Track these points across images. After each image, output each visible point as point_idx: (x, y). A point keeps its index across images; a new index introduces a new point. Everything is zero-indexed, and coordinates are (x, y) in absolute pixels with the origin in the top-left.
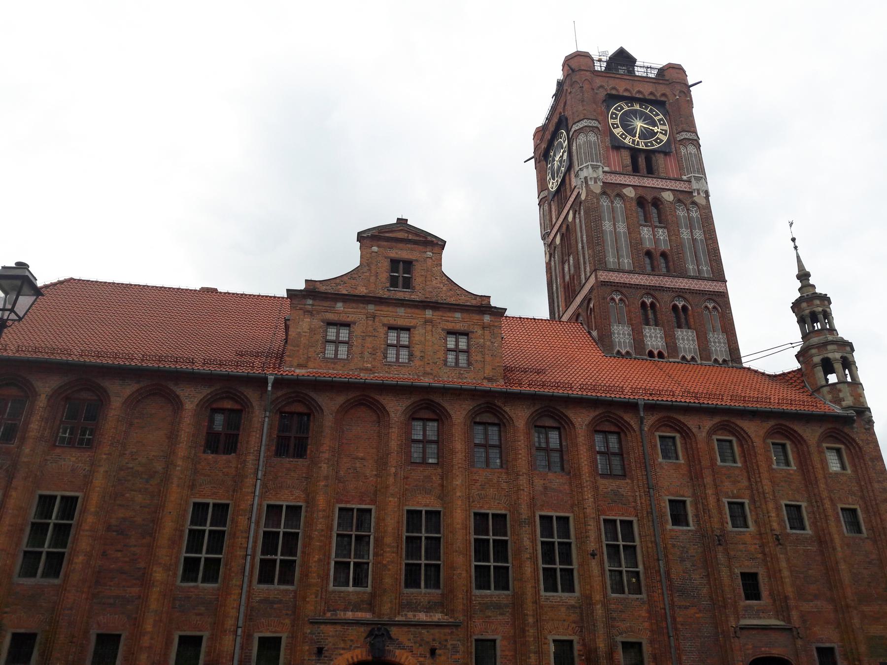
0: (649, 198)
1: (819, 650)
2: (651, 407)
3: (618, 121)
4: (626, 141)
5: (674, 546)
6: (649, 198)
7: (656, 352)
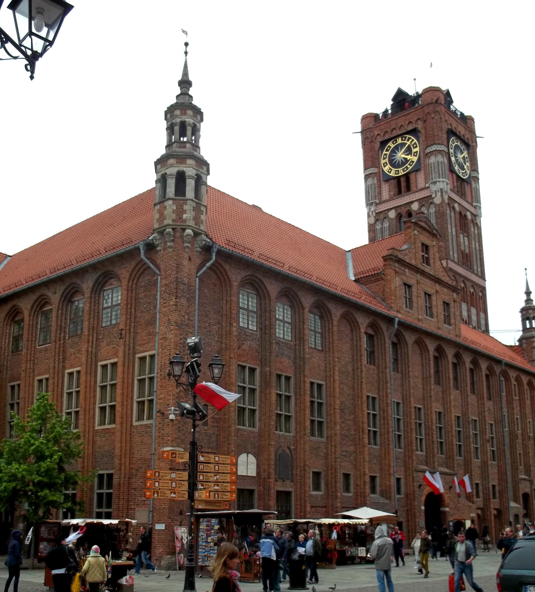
3: (387, 160)
4: (391, 174)
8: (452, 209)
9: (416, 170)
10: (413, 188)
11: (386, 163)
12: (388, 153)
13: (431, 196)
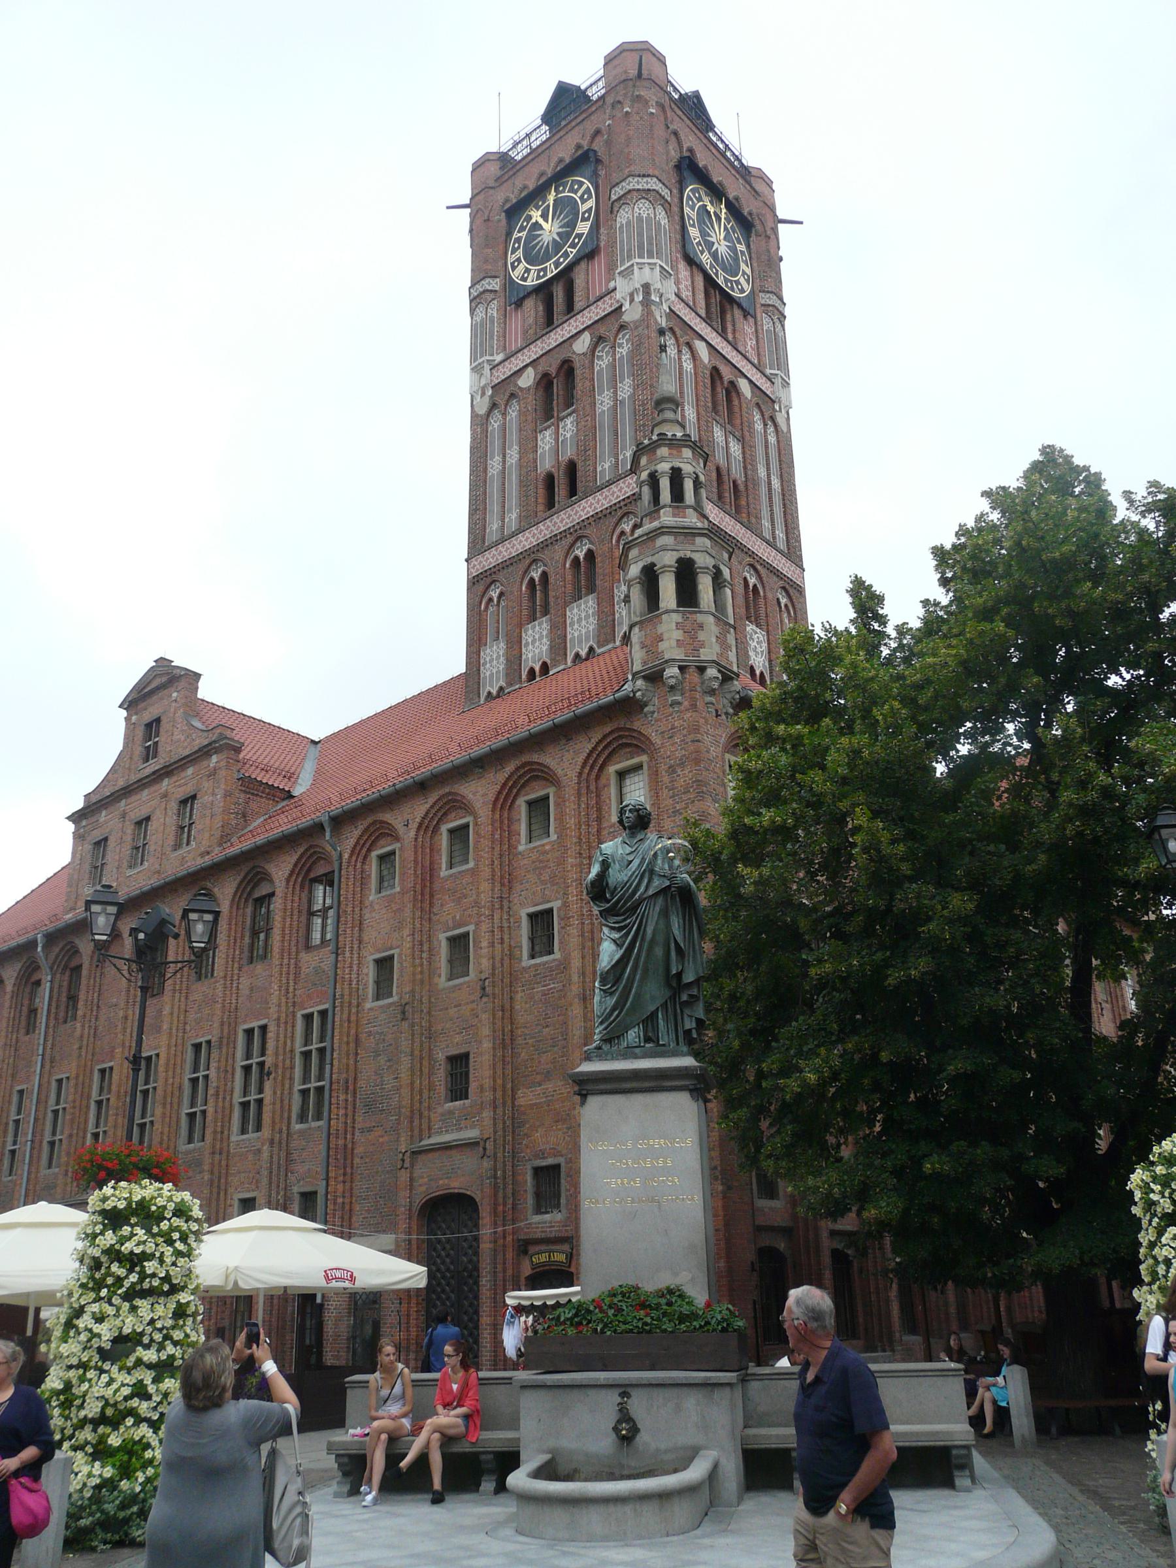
0: (553, 371)
1: (537, 1171)
2: (340, 821)
4: (528, 283)
5: (370, 1034)
6: (553, 371)
7: (537, 669)
8: (685, 350)
9: (589, 255)
10: (578, 305)
11: (519, 260)
12: (524, 234)
13: (621, 307)
